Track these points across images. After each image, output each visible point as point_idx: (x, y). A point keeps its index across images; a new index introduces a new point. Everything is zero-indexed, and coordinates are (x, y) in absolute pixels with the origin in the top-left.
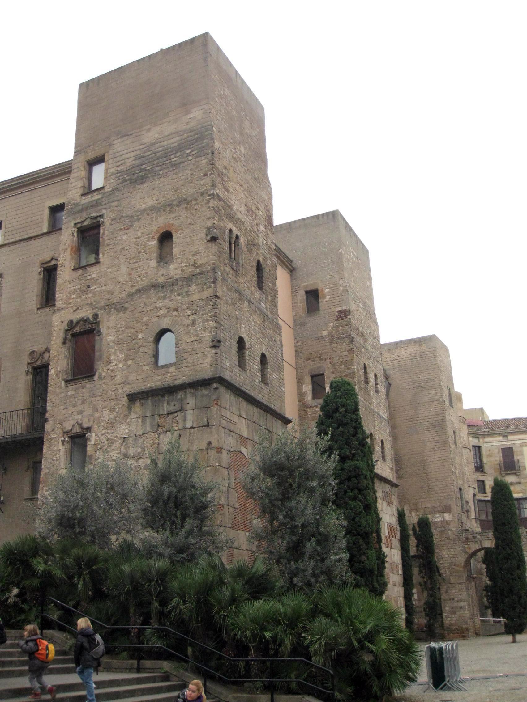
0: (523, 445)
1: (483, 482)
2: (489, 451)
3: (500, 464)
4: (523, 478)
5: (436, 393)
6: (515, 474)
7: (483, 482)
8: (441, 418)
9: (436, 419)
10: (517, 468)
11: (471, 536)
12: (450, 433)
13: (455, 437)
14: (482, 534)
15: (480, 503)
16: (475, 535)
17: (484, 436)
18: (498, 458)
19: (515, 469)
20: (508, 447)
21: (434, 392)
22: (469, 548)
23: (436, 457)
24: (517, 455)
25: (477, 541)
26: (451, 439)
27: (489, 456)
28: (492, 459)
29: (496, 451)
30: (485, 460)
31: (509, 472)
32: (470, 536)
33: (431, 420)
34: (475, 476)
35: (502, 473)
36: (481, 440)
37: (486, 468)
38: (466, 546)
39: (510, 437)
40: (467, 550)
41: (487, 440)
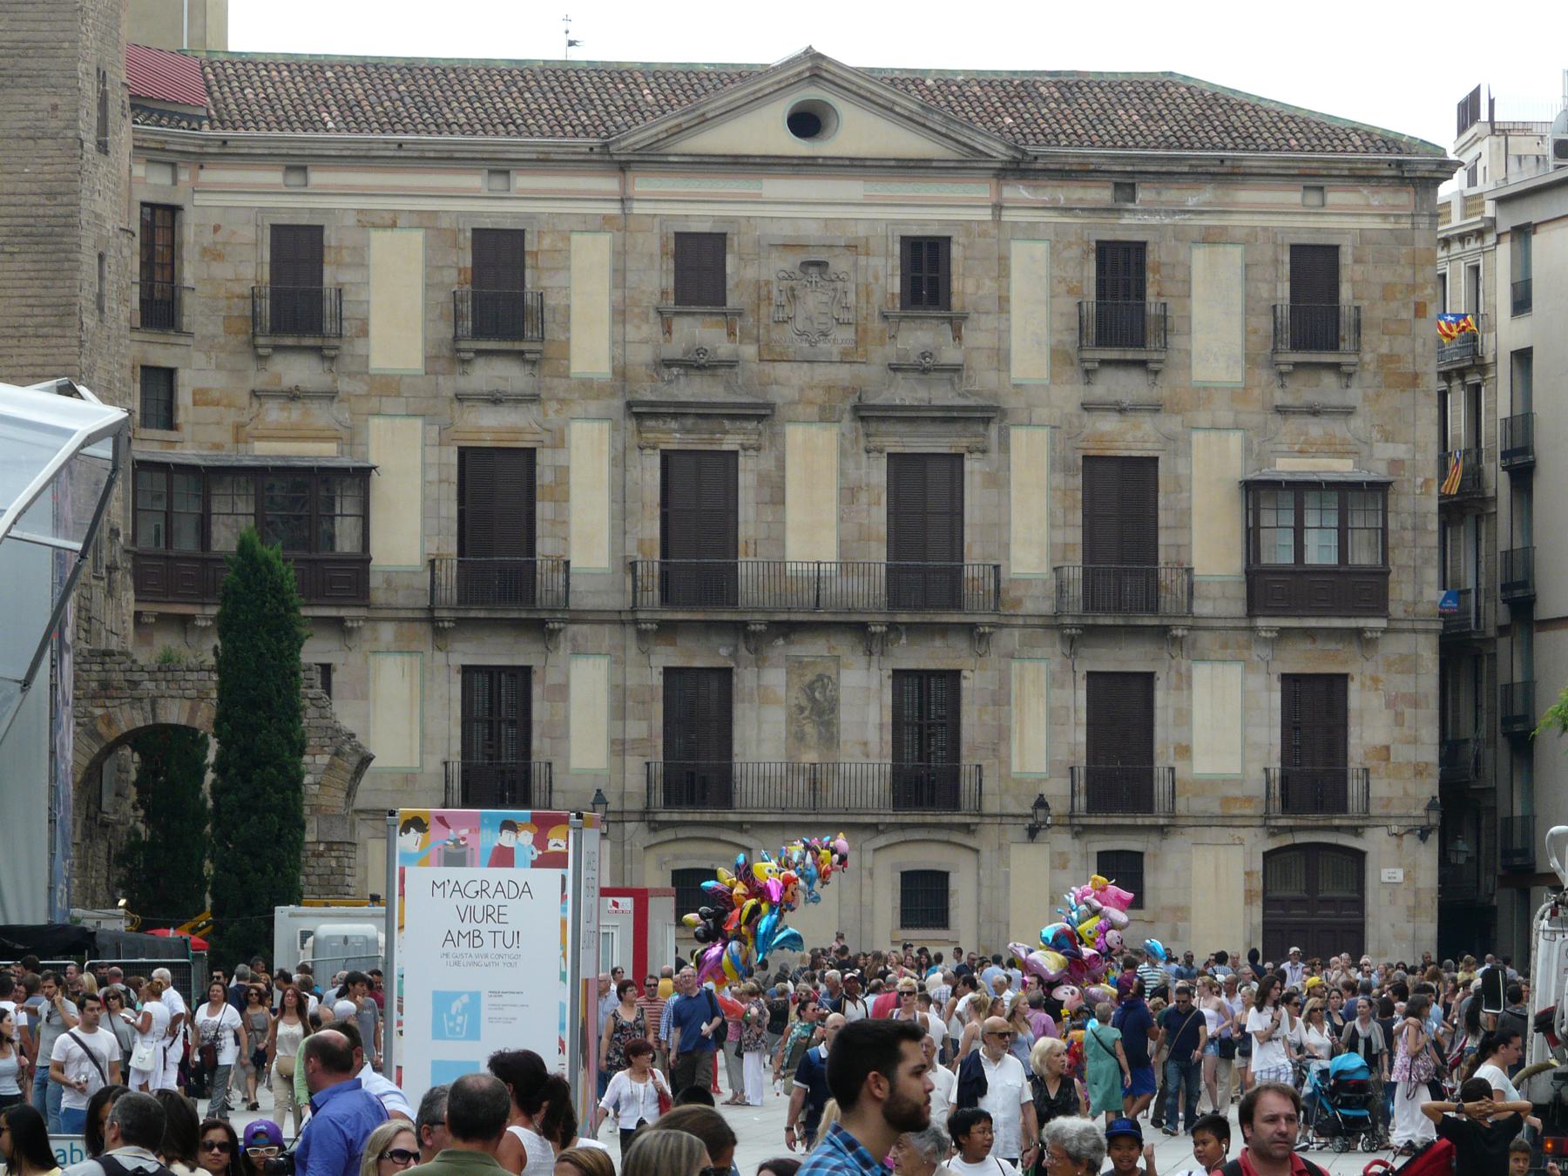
0: (368, 222)
1: (170, 374)
2: (217, 229)
3: (254, 296)
4: (350, 375)
5: (55, 107)
6: (317, 350)
7: (170, 374)
8: (61, 210)
9: (41, 211)
10: (328, 326)
11: (121, 676)
12: (88, 259)
13: (101, 277)
14: (160, 675)
15: (145, 475)
16: (136, 677)
17: (200, 159)
18: (251, 267)
19: (315, 327)
20: (304, 220)
21: (46, 101)
22: (110, 721)
23: (22, 361)
24: (340, 264)
25: (140, 699)
26: (86, 299)
27: (213, 254)
28: (221, 270)
29: (248, 233)
30: (189, 272)
31: (289, 341)
32: (117, 677)
33: (20, 211)
34: (135, 348)
35: (261, 341)
36: (184, 176)
37: (193, 310)
38: (99, 712)
39: (317, 178)
40: (102, 728)
41: (209, 176)
